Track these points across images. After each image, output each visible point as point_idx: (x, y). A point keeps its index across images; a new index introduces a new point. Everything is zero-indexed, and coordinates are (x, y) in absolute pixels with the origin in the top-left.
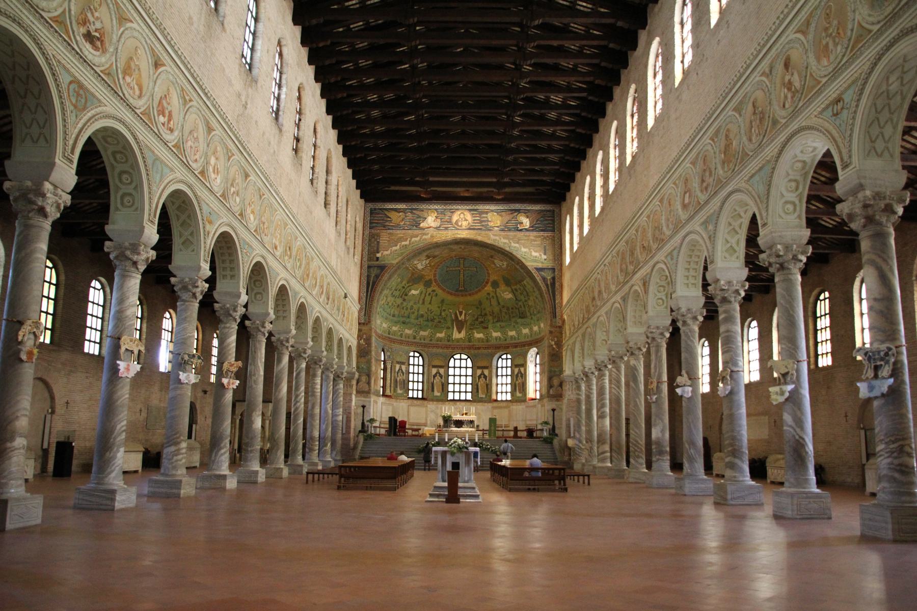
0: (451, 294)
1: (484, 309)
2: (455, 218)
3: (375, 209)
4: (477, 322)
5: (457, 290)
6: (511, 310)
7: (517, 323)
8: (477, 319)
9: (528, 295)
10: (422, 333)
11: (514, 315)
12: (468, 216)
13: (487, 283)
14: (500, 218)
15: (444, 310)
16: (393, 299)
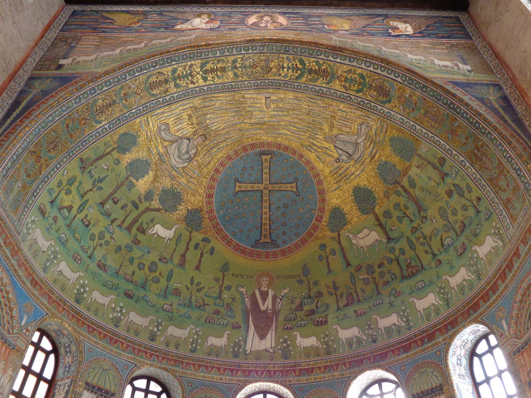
0: (243, 252)
1: (316, 283)
2: (252, 20)
3: (83, 11)
4: (301, 314)
5: (257, 243)
6: (378, 270)
7: (398, 294)
8: (300, 307)
9: (420, 208)
10: (173, 331)
11: (388, 277)
12: (282, 20)
13: (319, 219)
14: (349, 22)
15: (229, 288)
16: (104, 222)
